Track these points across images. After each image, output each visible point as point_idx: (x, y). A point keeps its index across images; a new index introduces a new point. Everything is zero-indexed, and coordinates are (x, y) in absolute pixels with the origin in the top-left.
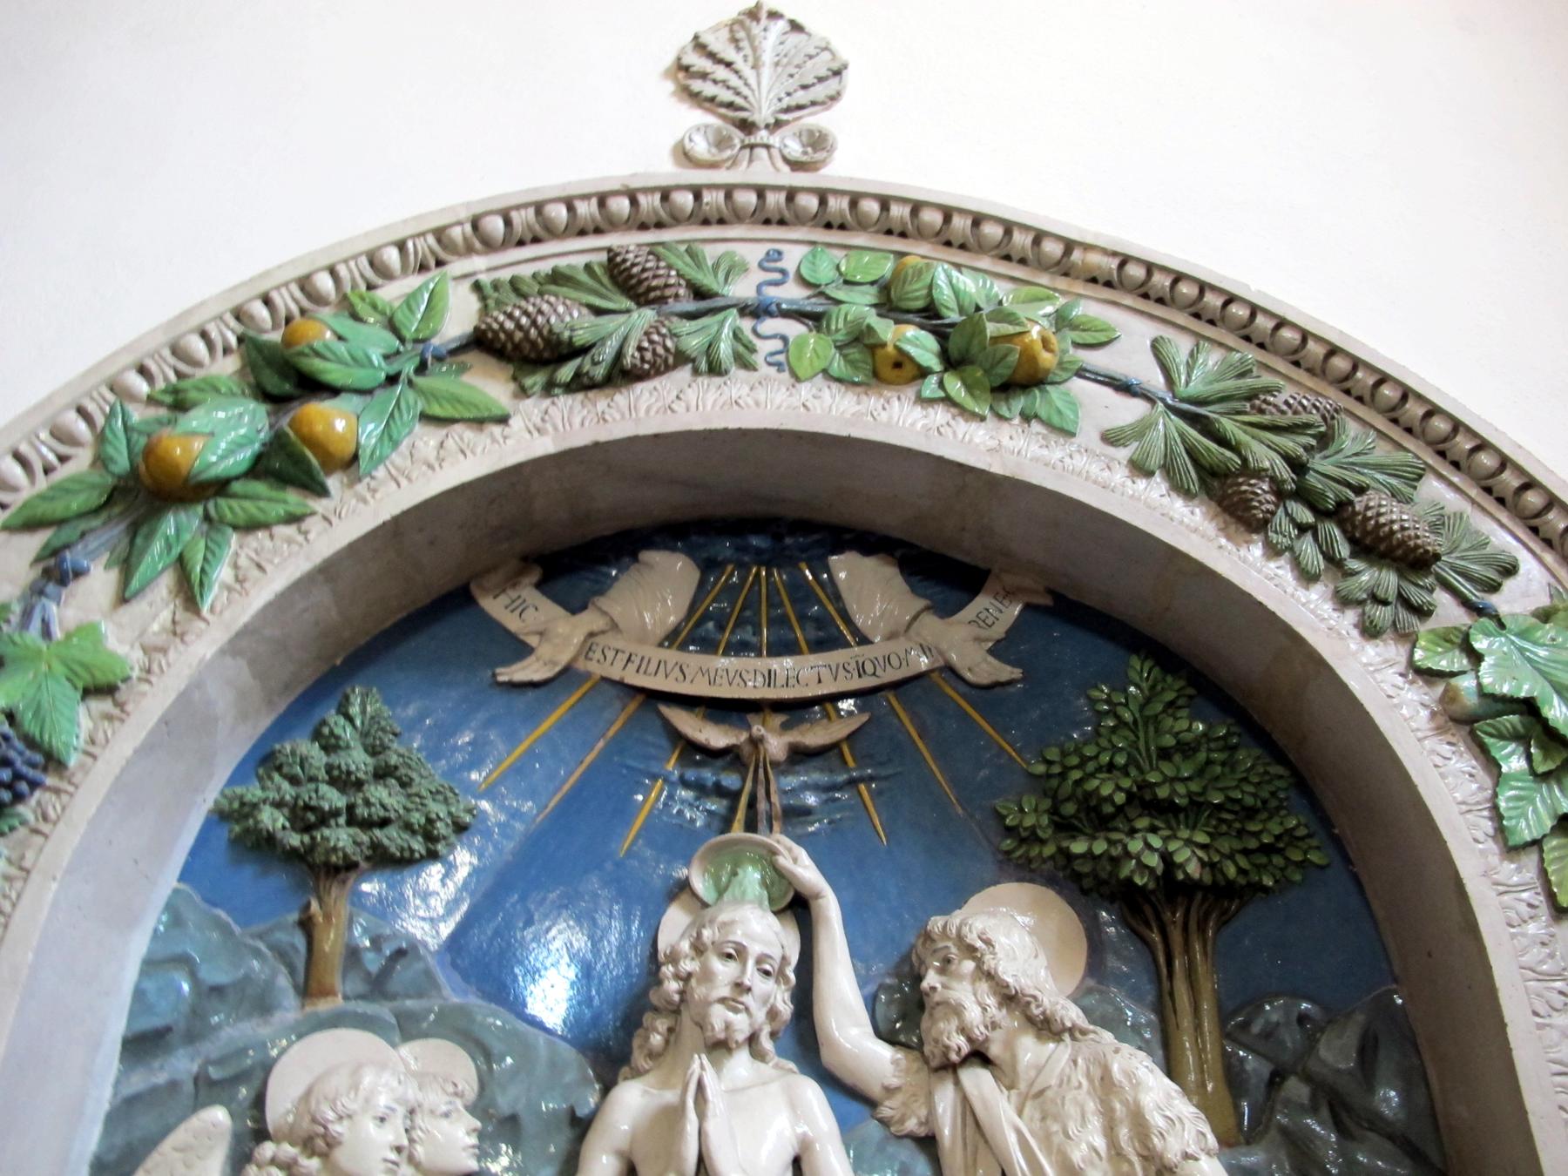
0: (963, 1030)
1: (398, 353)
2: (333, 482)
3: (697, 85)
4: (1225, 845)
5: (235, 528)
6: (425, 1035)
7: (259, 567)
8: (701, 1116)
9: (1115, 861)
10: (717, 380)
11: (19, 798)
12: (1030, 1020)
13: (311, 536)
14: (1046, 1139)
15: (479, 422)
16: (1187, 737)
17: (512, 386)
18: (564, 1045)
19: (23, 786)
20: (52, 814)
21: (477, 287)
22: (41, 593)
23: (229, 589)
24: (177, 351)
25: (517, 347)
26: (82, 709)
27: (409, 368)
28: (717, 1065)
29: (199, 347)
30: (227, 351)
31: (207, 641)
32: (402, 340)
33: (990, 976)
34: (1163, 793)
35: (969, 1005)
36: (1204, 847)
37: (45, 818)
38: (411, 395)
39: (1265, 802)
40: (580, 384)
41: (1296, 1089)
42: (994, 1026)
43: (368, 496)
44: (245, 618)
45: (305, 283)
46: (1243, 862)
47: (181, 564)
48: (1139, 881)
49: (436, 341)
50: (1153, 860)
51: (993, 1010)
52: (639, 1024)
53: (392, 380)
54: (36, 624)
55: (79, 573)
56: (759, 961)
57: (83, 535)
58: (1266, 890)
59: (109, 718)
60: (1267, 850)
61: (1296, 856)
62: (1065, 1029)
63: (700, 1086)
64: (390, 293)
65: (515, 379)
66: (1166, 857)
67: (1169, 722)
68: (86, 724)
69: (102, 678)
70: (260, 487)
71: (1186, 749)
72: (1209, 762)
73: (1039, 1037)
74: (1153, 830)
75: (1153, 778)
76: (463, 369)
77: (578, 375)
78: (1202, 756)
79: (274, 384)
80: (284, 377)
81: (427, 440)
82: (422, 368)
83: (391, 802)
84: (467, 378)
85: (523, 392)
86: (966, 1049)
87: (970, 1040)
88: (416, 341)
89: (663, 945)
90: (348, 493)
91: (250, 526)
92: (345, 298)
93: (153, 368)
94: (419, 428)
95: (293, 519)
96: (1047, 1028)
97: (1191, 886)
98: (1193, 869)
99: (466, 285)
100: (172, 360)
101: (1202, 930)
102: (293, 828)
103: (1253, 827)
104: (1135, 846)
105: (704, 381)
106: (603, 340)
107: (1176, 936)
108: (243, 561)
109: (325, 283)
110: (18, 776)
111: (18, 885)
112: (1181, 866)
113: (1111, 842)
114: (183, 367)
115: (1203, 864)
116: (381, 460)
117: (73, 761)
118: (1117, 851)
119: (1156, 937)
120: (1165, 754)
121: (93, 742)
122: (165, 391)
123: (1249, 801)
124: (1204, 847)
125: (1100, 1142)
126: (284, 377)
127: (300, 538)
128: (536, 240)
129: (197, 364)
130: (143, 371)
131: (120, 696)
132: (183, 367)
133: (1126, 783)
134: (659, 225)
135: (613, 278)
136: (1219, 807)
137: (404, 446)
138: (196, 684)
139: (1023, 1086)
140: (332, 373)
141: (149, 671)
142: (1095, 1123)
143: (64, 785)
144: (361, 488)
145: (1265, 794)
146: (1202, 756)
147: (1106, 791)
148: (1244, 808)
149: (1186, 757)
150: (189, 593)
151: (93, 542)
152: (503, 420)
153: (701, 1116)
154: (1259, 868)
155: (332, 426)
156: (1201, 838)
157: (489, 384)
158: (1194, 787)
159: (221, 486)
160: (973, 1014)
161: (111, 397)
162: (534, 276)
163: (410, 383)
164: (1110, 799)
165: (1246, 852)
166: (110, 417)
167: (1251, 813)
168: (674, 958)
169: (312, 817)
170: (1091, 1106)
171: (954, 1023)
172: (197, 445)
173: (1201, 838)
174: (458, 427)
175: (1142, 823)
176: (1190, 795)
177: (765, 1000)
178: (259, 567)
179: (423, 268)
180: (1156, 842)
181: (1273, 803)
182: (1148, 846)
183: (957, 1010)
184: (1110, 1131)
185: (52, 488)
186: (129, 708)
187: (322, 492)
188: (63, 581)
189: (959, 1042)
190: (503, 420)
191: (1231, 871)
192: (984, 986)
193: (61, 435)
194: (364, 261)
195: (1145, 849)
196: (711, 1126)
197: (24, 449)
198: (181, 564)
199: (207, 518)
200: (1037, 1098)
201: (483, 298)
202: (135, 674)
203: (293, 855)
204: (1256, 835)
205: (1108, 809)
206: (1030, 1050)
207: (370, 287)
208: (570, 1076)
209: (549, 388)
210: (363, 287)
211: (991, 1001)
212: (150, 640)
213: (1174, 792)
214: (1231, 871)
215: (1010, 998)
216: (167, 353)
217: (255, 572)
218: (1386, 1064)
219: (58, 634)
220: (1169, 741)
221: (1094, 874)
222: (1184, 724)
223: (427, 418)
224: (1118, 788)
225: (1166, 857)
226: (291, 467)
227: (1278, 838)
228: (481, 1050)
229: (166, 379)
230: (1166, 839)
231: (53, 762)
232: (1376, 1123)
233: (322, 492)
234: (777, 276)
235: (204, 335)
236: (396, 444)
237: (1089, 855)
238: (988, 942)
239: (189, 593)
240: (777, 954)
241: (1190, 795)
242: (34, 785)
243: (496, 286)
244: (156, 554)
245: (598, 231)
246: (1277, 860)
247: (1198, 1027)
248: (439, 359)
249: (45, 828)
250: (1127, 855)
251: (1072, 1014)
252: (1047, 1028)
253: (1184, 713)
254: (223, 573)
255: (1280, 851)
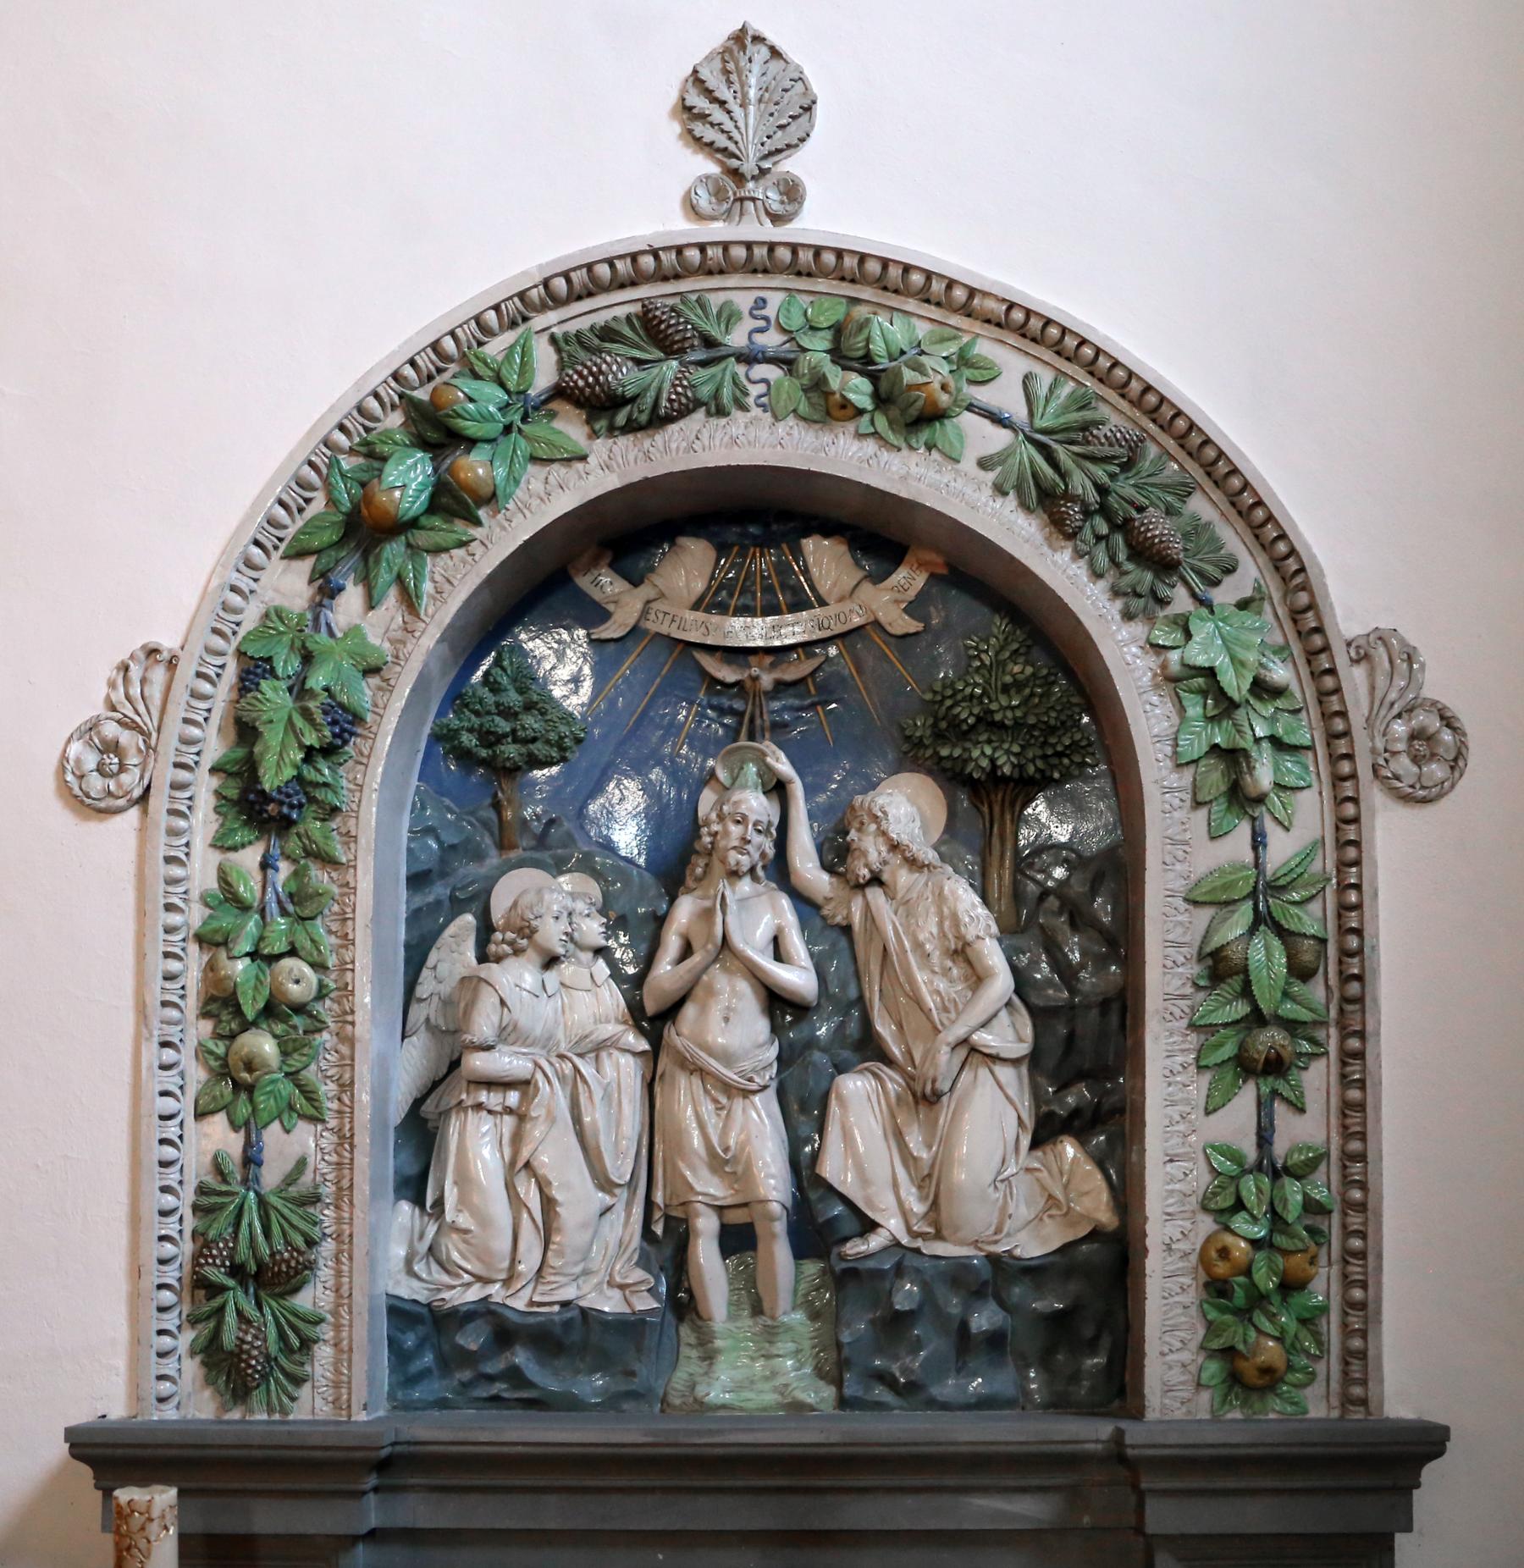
0: (867, 865)
1: (508, 405)
2: (482, 513)
3: (700, 129)
4: (1030, 755)
5: (428, 551)
6: (569, 871)
7: (449, 581)
8: (724, 913)
9: (966, 761)
10: (723, 421)
11: (346, 742)
12: (906, 859)
13: (477, 558)
14: (907, 927)
15: (568, 461)
16: (1021, 677)
17: (586, 429)
18: (646, 874)
19: (346, 735)
20: (366, 752)
21: (553, 340)
22: (320, 605)
23: (435, 599)
24: (360, 409)
25: (587, 399)
26: (364, 684)
27: (517, 418)
28: (732, 885)
29: (373, 404)
30: (394, 407)
31: (429, 637)
32: (508, 392)
33: (884, 834)
34: (998, 717)
35: (871, 850)
36: (1016, 755)
37: (362, 754)
38: (522, 442)
39: (1063, 723)
40: (631, 427)
41: (1053, 902)
42: (885, 863)
43: (506, 524)
44: (447, 620)
45: (435, 346)
46: (1040, 763)
47: (400, 580)
48: (975, 776)
49: (532, 392)
50: (985, 763)
51: (884, 854)
52: (689, 862)
53: (508, 429)
54: (323, 629)
55: (341, 589)
56: (755, 824)
57: (337, 562)
58: (1056, 781)
59: (380, 689)
60: (1060, 755)
61: (1077, 759)
62: (924, 866)
63: (723, 897)
64: (495, 348)
65: (588, 422)
66: (993, 761)
67: (1010, 665)
68: (368, 692)
69: (373, 661)
70: (437, 522)
71: (1018, 685)
72: (1032, 695)
73: (911, 870)
74: (989, 742)
75: (994, 706)
76: (552, 415)
77: (629, 420)
78: (1027, 691)
79: (432, 435)
80: (437, 432)
81: (535, 477)
82: (524, 419)
83: (536, 726)
84: (557, 424)
85: (594, 434)
86: (868, 876)
87: (871, 871)
88: (519, 393)
89: (700, 814)
90: (493, 522)
91: (438, 550)
92: (464, 355)
93: (348, 424)
94: (531, 468)
95: (462, 544)
96: (913, 863)
97: (1005, 780)
98: (1007, 770)
99: (545, 337)
100: (361, 420)
101: (1013, 804)
102: (482, 746)
103: (1053, 740)
104: (976, 753)
105: (714, 421)
106: (646, 389)
107: (997, 809)
108: (438, 578)
109: (449, 345)
110: (343, 730)
111: (358, 794)
112: (1001, 767)
113: (965, 750)
114: (367, 423)
115: (1014, 766)
116: (510, 496)
117: (369, 718)
118: (966, 756)
119: (985, 809)
120: (1006, 689)
121: (376, 705)
122: (360, 444)
123: (1052, 722)
124: (1016, 755)
125: (935, 930)
126: (437, 432)
127: (470, 559)
128: (590, 294)
129: (377, 420)
130: (342, 428)
131: (385, 673)
132: (367, 423)
133: (976, 711)
134: (677, 277)
135: (646, 329)
136: (1033, 726)
137: (523, 484)
138: (426, 665)
139: (899, 896)
140: (471, 428)
141: (397, 657)
142: (934, 919)
143: (365, 733)
144: (500, 516)
145: (1063, 717)
146: (1027, 691)
147: (963, 716)
148: (1050, 727)
149: (1018, 692)
150: (410, 600)
151: (343, 568)
152: (583, 458)
153: (724, 913)
154: (1053, 767)
155: (477, 474)
156: (1016, 749)
157: (570, 427)
158: (1019, 713)
159: (414, 523)
160: (873, 857)
161: (328, 453)
162: (592, 328)
163: (520, 431)
164: (965, 720)
165: (1044, 757)
166: (329, 466)
167: (1052, 730)
168: (707, 823)
169: (492, 738)
170: (933, 910)
171: (862, 861)
172: (397, 494)
173: (1016, 749)
174: (556, 466)
175: (984, 737)
176: (1015, 718)
177: (759, 847)
178: (449, 581)
179: (513, 324)
180: (988, 751)
181: (1069, 723)
182: (983, 753)
183: (865, 854)
184: (940, 924)
185: (306, 525)
186: (392, 682)
187: (478, 523)
188: (332, 597)
189: (864, 873)
190: (583, 458)
191: (1031, 769)
192: (881, 839)
193: (303, 484)
194: (473, 324)
195: (981, 754)
196: (730, 919)
197: (285, 497)
198: (400, 580)
199: (409, 545)
200: (906, 907)
201: (559, 351)
202: (389, 659)
203: (483, 762)
204: (1053, 746)
205: (965, 727)
206: (904, 878)
207: (480, 344)
208: (653, 892)
209: (612, 430)
210: (475, 344)
211: (883, 849)
212: (392, 634)
213: (1005, 717)
214: (1031, 769)
215: (895, 847)
216: (355, 413)
217: (447, 587)
218: (1109, 885)
219: (339, 635)
220: (1008, 679)
221: (952, 769)
222: (1017, 669)
223: (534, 459)
224: (971, 714)
225: (993, 761)
226: (454, 503)
227: (1067, 747)
228: (597, 875)
229: (359, 435)
230: (995, 750)
231: (358, 719)
232: (1094, 924)
233: (478, 523)
234: (762, 323)
235: (376, 395)
236: (517, 482)
237: (950, 757)
238: (885, 813)
239: (410, 600)
240: (765, 819)
241: (1015, 718)
242: (352, 734)
243: (566, 335)
244: (384, 576)
245: (633, 284)
246: (1066, 761)
247: (1002, 865)
248: (536, 408)
249: (365, 761)
250: (971, 759)
251: (931, 856)
252: (913, 863)
253: (1021, 659)
254: (427, 587)
255: (1068, 756)
